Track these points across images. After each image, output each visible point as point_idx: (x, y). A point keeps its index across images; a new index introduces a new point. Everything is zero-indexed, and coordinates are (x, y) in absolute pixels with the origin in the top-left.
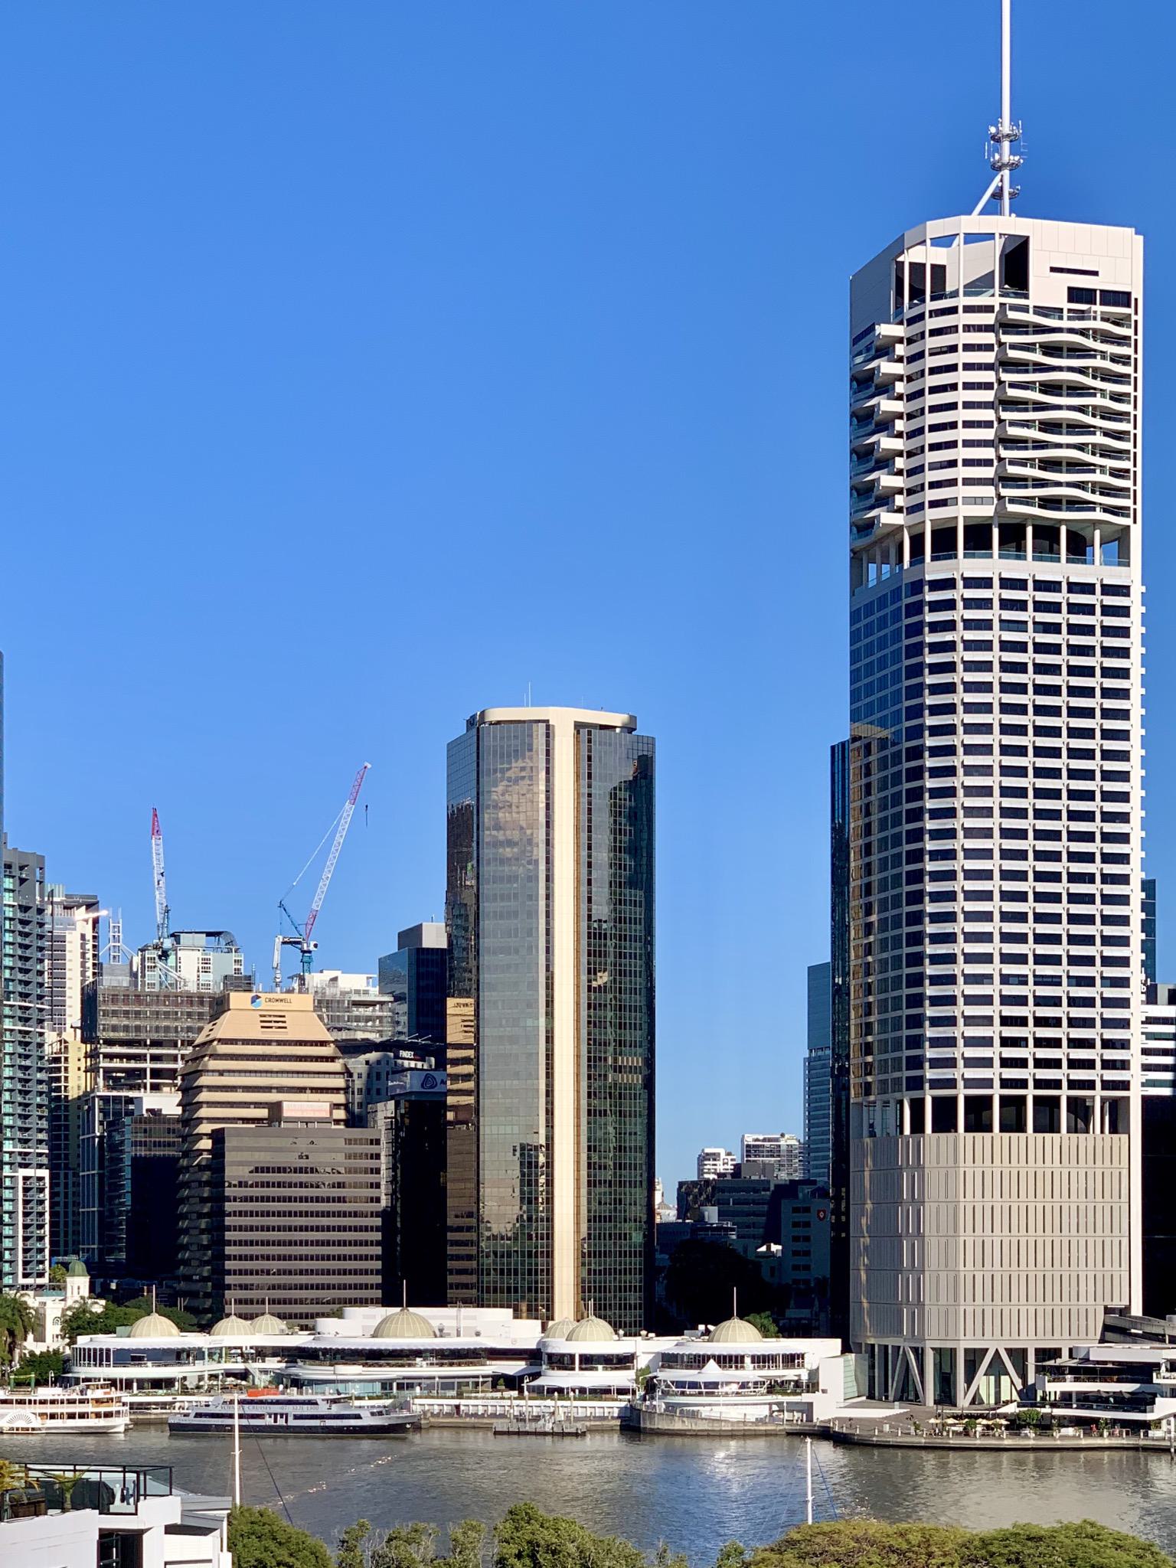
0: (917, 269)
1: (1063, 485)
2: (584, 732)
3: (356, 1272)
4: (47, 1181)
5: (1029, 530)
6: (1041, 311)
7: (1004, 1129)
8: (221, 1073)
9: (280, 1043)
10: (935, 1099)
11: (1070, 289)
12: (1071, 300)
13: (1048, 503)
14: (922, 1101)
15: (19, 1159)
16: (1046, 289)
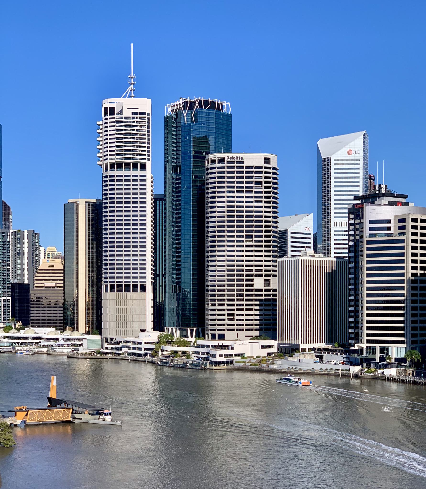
0: (106, 109)
1: (129, 154)
2: (87, 204)
3: (42, 320)
4: (10, 300)
5: (123, 164)
6: (125, 118)
8: (39, 277)
9: (52, 270)
10: (110, 285)
11: (132, 113)
12: (132, 115)
13: (125, 158)
14: (108, 285)
15: (2, 295)
16: (127, 113)
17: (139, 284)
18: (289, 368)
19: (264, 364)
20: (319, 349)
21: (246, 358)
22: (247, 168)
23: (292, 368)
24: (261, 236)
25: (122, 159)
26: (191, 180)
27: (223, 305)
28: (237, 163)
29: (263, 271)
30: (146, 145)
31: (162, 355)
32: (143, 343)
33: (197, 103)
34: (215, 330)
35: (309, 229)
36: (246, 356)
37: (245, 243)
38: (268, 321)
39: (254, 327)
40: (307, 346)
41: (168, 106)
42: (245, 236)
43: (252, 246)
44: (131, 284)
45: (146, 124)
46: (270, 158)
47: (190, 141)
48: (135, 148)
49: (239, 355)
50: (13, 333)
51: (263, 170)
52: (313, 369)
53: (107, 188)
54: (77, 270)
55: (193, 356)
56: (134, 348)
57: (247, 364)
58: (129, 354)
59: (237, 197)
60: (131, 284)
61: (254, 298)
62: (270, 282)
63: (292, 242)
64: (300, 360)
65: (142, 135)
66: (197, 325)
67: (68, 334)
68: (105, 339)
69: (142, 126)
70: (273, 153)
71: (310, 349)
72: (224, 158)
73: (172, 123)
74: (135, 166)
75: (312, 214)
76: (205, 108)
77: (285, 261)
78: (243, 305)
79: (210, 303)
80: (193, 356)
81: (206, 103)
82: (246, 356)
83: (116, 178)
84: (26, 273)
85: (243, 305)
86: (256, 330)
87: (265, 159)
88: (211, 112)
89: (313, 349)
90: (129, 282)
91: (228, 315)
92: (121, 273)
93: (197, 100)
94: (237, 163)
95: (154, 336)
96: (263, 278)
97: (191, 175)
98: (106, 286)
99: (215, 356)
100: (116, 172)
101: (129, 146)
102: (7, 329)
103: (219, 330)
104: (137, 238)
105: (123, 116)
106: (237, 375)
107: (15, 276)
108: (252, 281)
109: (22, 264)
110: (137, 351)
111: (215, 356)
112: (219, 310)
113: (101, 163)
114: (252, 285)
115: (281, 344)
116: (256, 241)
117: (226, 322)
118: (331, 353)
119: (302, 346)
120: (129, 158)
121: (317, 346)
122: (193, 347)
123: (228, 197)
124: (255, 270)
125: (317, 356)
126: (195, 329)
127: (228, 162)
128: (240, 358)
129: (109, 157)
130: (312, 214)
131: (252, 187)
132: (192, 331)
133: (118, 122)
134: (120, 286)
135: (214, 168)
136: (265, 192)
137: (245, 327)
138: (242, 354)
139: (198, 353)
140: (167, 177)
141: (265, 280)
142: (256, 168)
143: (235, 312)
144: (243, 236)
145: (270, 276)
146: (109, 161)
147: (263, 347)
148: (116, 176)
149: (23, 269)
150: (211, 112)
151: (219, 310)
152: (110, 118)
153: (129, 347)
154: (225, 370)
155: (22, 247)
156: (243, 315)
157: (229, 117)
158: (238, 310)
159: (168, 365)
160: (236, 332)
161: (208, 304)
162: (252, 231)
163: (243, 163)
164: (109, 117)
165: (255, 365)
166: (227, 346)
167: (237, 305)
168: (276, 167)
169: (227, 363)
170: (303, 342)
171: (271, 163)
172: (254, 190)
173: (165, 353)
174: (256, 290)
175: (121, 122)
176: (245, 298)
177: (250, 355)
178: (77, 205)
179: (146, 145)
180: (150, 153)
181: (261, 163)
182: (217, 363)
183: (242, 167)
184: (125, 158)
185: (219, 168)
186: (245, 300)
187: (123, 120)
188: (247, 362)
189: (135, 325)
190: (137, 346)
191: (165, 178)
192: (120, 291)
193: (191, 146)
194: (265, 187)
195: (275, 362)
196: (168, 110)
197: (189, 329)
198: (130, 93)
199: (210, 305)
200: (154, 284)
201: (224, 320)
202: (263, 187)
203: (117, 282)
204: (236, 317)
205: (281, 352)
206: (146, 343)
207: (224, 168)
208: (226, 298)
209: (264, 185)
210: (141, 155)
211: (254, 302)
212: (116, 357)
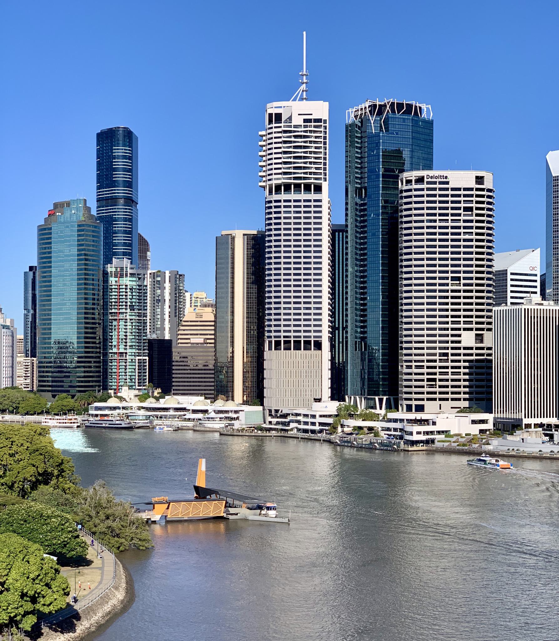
0: (270, 115)
1: (300, 173)
2: (246, 237)
3: (188, 386)
4: (147, 360)
5: (293, 186)
6: (295, 126)
7: (285, 349)
8: (184, 330)
9: (201, 321)
10: (275, 341)
12: (304, 122)
13: (295, 178)
15: (137, 354)
17: (312, 340)
18: (509, 449)
19: (475, 443)
20: (549, 426)
21: (452, 436)
22: (453, 189)
23: (513, 450)
24: (471, 278)
25: (290, 178)
26: (379, 206)
27: (422, 367)
28: (440, 183)
29: (474, 323)
30: (322, 161)
31: (343, 431)
32: (317, 416)
33: (388, 106)
34: (411, 399)
35: (535, 269)
36: (452, 433)
37: (450, 288)
38: (480, 388)
39: (462, 396)
40: (532, 421)
41: (350, 111)
42: (450, 278)
43: (459, 291)
44: (302, 340)
45: (322, 135)
46: (482, 177)
47: (379, 155)
48: (308, 165)
49: (443, 432)
50: (150, 403)
51: (474, 192)
52: (540, 451)
53: (271, 216)
54: (233, 322)
55: (382, 433)
56: (306, 423)
57: (453, 444)
58: (299, 430)
59: (440, 227)
60: (302, 340)
61: (462, 358)
62: (482, 337)
63: (512, 286)
64: (523, 439)
65: (316, 148)
66: (387, 393)
67: (220, 404)
68: (268, 411)
69: (316, 137)
70: (487, 171)
71: (536, 425)
72: (423, 177)
73: (355, 133)
74: (308, 188)
75: (539, 249)
76: (398, 113)
77: (503, 310)
78: (447, 367)
79: (405, 364)
80: (382, 433)
81: (400, 106)
82: (452, 433)
83: (283, 204)
84: (167, 326)
85: (447, 367)
86: (465, 399)
87: (477, 177)
88: (406, 117)
89: (541, 425)
90: (300, 337)
91: (428, 380)
92: (289, 326)
93: (388, 103)
94: (440, 183)
95: (332, 407)
96: (474, 332)
97: (379, 200)
98: (270, 342)
99: (411, 433)
100: (283, 196)
101: (300, 163)
102: (142, 398)
103: (416, 400)
104: (310, 280)
105: (292, 124)
106: (440, 459)
107: (154, 329)
108: (459, 336)
109: (163, 314)
110: (309, 427)
111: (411, 433)
112: (416, 374)
113: (264, 184)
114: (459, 342)
115: (498, 418)
116: (465, 285)
117: (426, 389)
119: (526, 421)
120: (300, 178)
121: (545, 421)
122: (382, 420)
123: (428, 227)
124: (464, 322)
125: (546, 435)
126: (385, 398)
127: (428, 183)
128: (444, 436)
129: (274, 177)
130: (539, 249)
131: (459, 215)
132: (381, 401)
133: (285, 132)
134: (287, 342)
135: (410, 190)
136: (477, 221)
137: (450, 396)
138: (446, 432)
139: (388, 429)
140: (349, 201)
141: (476, 335)
142: (465, 189)
143: (438, 377)
144: (447, 278)
145: (483, 329)
146: (274, 182)
147: (474, 422)
148: (282, 201)
149: (163, 320)
150: (406, 117)
151: (416, 374)
152: (275, 127)
153: (299, 422)
154: (424, 452)
155: (163, 293)
156: (447, 380)
157: (429, 124)
158: (441, 373)
159: (349, 444)
160: (438, 402)
161: (402, 366)
162: (459, 272)
163: (447, 183)
164: (274, 125)
165: (464, 445)
166: (427, 421)
167: (440, 367)
168: (491, 188)
169: (427, 442)
170: (527, 416)
171: (485, 182)
172: (462, 218)
173: (346, 429)
174: (465, 348)
175: (290, 132)
176: (451, 358)
177: (457, 432)
178: (233, 238)
179: (322, 161)
180: (327, 172)
181: (472, 184)
182: (414, 443)
183: (447, 189)
184: (295, 178)
185: (416, 190)
186: (450, 361)
187: (292, 129)
188: (454, 442)
189: (307, 393)
190: (310, 420)
191: (347, 204)
192: (288, 348)
193: (379, 161)
194: (477, 215)
195: (490, 442)
196: (350, 116)
197: (377, 398)
198: (302, 95)
199: (405, 367)
200: (332, 340)
201: (423, 387)
202: (474, 215)
203: (284, 337)
204: (438, 383)
205: (498, 429)
206: (321, 416)
207: (423, 190)
208: (425, 358)
209: (475, 212)
210: (315, 173)
211: (462, 364)
212: (282, 434)
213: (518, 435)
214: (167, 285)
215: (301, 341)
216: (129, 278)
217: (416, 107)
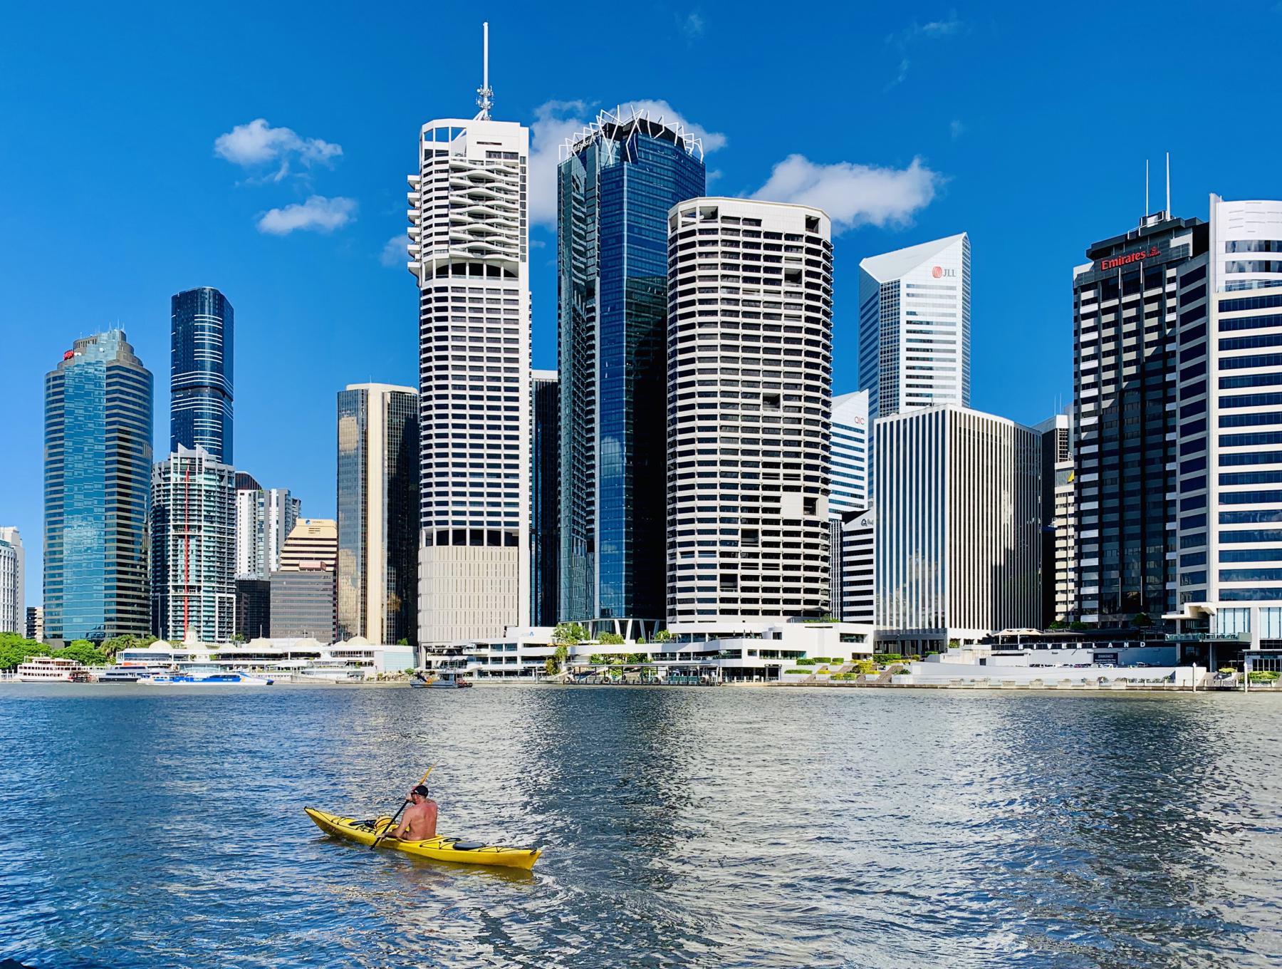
21: (809, 663)
22: (768, 235)
36: (809, 656)
96: (802, 494)
108: (777, 499)
118: (1049, 646)
119: (952, 633)
141: (806, 499)
142: (789, 237)
147: (845, 637)
170: (954, 625)
181: (801, 229)
213: (950, 659)
214: (274, 510)
215: (482, 531)
216: (203, 476)
217: (680, 139)
